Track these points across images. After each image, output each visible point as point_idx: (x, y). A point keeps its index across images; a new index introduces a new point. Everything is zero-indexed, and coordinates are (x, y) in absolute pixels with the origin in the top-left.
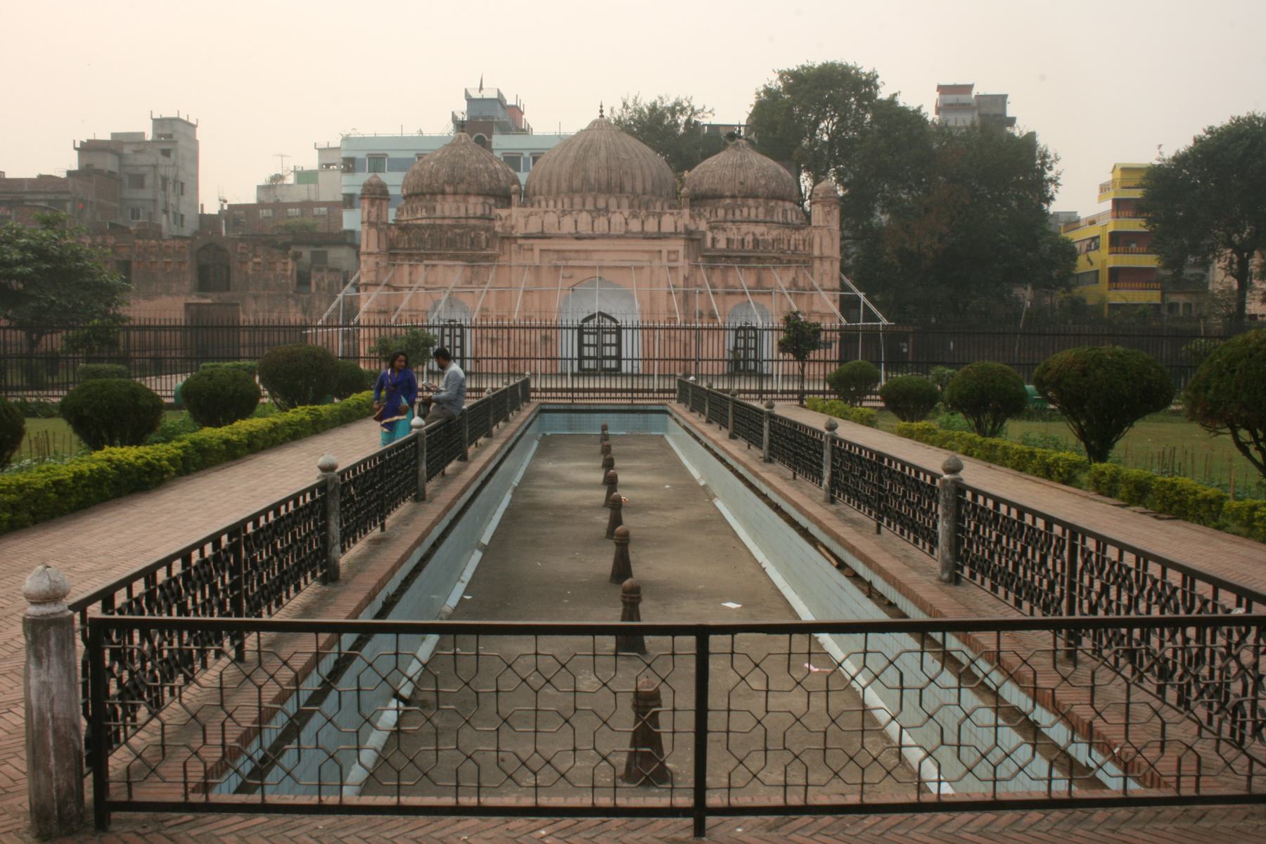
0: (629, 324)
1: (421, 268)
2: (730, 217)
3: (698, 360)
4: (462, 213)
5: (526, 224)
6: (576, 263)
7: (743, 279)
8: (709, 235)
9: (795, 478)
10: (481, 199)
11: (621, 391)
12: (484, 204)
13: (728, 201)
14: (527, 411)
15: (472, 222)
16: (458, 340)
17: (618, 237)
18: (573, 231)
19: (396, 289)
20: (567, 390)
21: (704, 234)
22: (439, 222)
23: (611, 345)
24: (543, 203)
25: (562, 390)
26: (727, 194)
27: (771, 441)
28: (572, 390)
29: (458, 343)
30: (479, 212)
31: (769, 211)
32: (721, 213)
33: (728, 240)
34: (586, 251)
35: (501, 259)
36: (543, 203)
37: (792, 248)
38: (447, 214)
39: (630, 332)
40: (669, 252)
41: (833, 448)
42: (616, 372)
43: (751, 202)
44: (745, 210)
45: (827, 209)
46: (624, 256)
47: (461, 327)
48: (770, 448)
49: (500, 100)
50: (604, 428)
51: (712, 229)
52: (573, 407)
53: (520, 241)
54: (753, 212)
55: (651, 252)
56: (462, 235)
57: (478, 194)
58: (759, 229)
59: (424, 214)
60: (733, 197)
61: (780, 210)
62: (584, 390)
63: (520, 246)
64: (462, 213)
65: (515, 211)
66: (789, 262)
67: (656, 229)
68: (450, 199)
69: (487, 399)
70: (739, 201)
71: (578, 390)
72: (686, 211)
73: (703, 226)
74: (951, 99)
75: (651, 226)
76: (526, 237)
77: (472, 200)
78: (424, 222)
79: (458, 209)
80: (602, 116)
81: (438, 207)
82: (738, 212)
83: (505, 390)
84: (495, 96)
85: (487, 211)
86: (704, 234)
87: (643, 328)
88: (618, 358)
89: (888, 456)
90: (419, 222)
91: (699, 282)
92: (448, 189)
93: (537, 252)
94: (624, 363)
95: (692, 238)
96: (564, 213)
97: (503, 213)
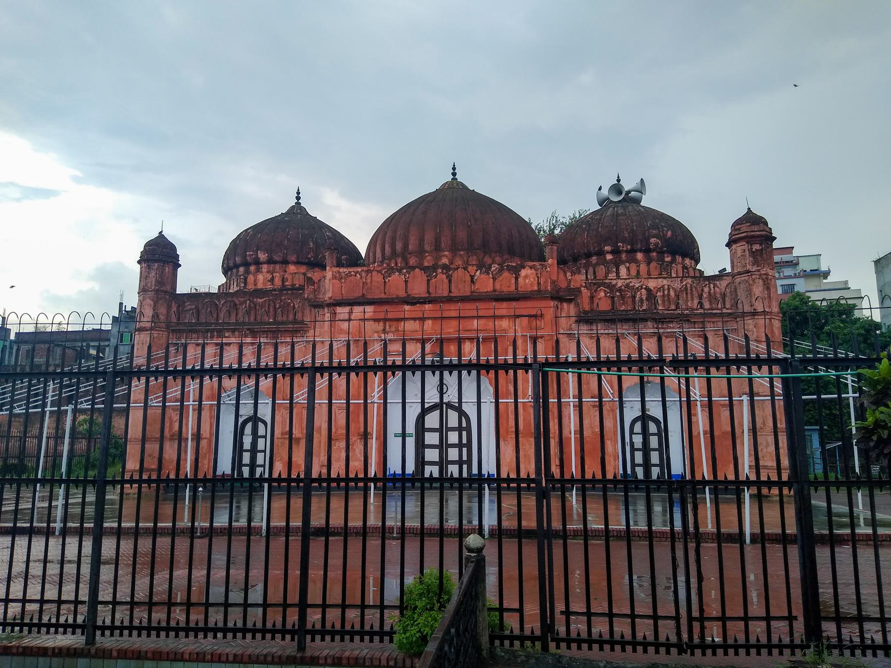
2: (612, 276)
10: (303, 269)
13: (609, 257)
17: (463, 299)
30: (299, 281)
37: (707, 305)
43: (639, 256)
45: (756, 247)
56: (262, 306)
57: (298, 263)
59: (236, 289)
64: (278, 282)
67: (513, 288)
68: (265, 268)
70: (624, 256)
75: (506, 283)
77: (292, 268)
80: (454, 179)
81: (251, 278)
82: (623, 271)
86: (578, 290)
92: (262, 256)
97: (315, 275)
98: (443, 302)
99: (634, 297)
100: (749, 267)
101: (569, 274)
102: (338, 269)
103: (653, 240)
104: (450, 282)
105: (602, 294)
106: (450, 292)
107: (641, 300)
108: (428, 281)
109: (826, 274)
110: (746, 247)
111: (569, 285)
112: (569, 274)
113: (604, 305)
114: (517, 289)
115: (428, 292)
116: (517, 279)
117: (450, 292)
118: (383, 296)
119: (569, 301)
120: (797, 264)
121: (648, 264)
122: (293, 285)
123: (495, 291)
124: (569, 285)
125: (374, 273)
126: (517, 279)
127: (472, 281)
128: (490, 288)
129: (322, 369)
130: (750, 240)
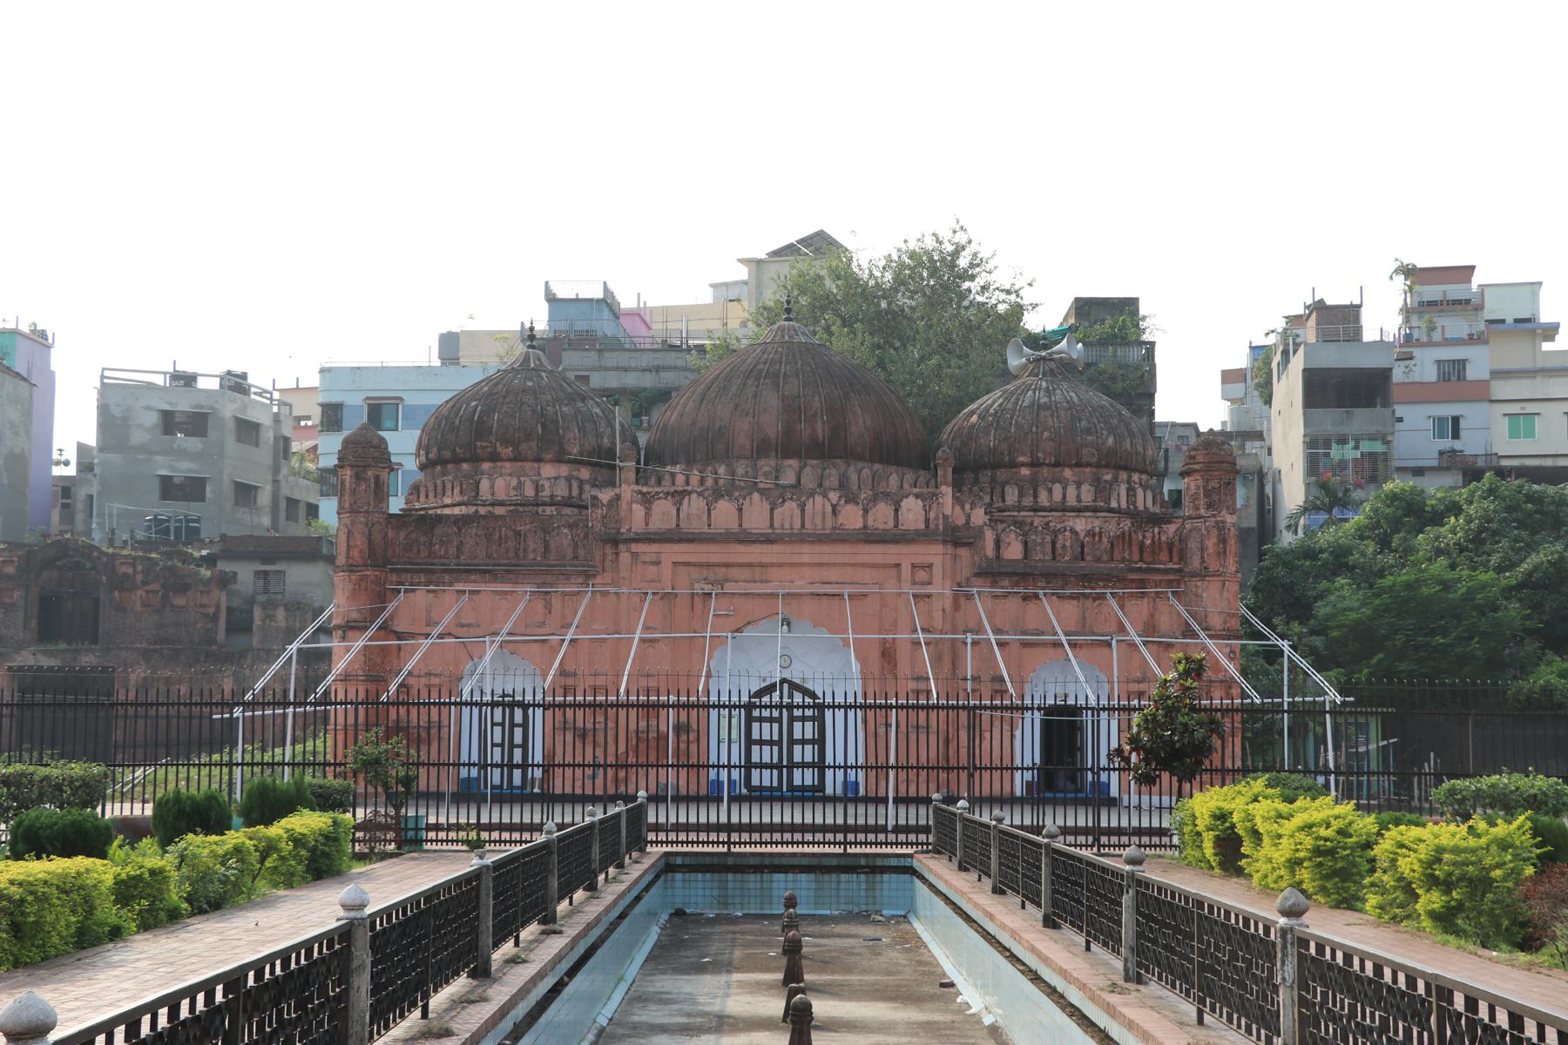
0: (840, 700)
1: (449, 598)
3: (973, 769)
4: (529, 491)
5: (648, 515)
6: (741, 588)
7: (1054, 614)
8: (989, 536)
9: (1200, 1021)
10: (564, 470)
11: (824, 829)
12: (568, 479)
13: (1025, 471)
14: (636, 869)
15: (549, 510)
16: (518, 732)
18: (734, 526)
19: (400, 636)
20: (718, 828)
21: (979, 532)
22: (482, 511)
23: (803, 742)
24: (680, 479)
25: (708, 828)
26: (1021, 459)
27: (1140, 935)
28: (729, 828)
29: (518, 739)
30: (561, 491)
31: (1102, 490)
32: (1012, 495)
33: (1026, 543)
34: (761, 565)
35: (598, 580)
36: (680, 479)
38: (501, 496)
39: (840, 714)
40: (914, 566)
41: (1302, 958)
42: (814, 795)
43: (1068, 473)
44: (1057, 488)
46: (832, 574)
47: (525, 706)
48: (1138, 950)
49: (607, 303)
50: (791, 902)
51: (993, 522)
52: (730, 861)
53: (635, 547)
54: (1072, 492)
55: (884, 566)
57: (560, 461)
58: (1081, 525)
59: (458, 498)
60: (1034, 464)
61: (1123, 488)
62: (750, 828)
63: (635, 555)
64: (529, 491)
65: (627, 491)
66: (1142, 584)
67: (891, 524)
69: (545, 846)
71: (741, 828)
72: (947, 490)
73: (979, 517)
74: (1432, 292)
75: (882, 516)
76: (649, 538)
77: (548, 470)
78: (456, 511)
79: (520, 486)
81: (485, 484)
83: (591, 826)
84: (600, 295)
85: (575, 492)
86: (980, 530)
87: (864, 707)
88: (820, 766)
89: (1462, 987)
90: (447, 511)
91: (972, 625)
93: (666, 567)
94: (829, 773)
95: (957, 537)
96: (718, 494)
97: (605, 496)
98: (791, 542)
99: (1054, 543)
100: (1202, 512)
101: (967, 506)
102: (637, 488)
103: (1085, 451)
104: (803, 511)
105: (1013, 536)
106: (803, 526)
107: (1064, 547)
108: (772, 510)
109: (1551, 331)
110: (1200, 483)
111: (968, 522)
112: (967, 506)
113: (1014, 551)
114: (896, 526)
115: (772, 526)
116: (896, 511)
117: (803, 526)
118: (706, 530)
119: (969, 545)
120: (1479, 308)
121: (1079, 485)
122: (552, 496)
123: (865, 527)
124: (968, 522)
125: (694, 496)
126: (896, 511)
127: (834, 512)
128: (859, 524)
129: (851, 707)
130: (1207, 470)
